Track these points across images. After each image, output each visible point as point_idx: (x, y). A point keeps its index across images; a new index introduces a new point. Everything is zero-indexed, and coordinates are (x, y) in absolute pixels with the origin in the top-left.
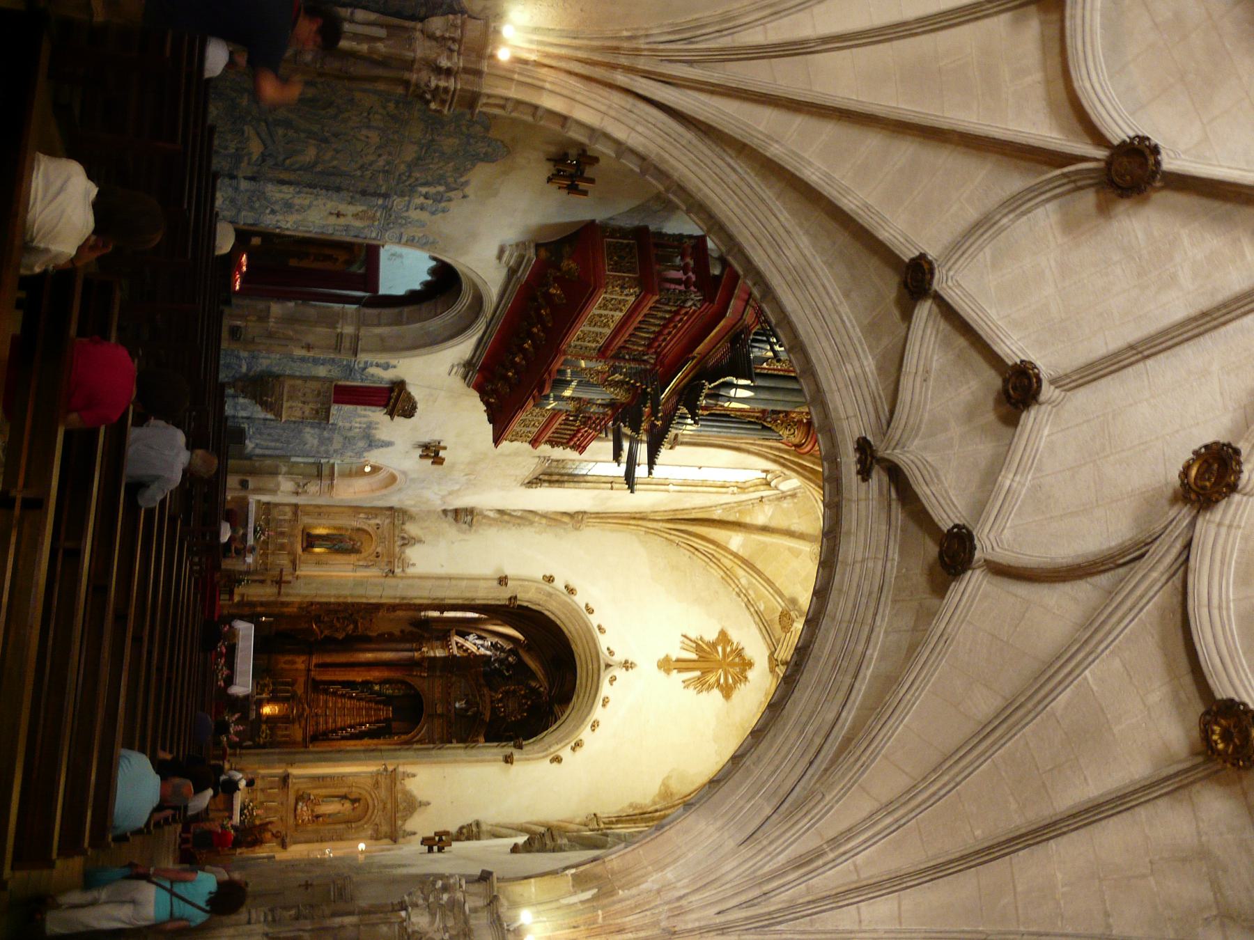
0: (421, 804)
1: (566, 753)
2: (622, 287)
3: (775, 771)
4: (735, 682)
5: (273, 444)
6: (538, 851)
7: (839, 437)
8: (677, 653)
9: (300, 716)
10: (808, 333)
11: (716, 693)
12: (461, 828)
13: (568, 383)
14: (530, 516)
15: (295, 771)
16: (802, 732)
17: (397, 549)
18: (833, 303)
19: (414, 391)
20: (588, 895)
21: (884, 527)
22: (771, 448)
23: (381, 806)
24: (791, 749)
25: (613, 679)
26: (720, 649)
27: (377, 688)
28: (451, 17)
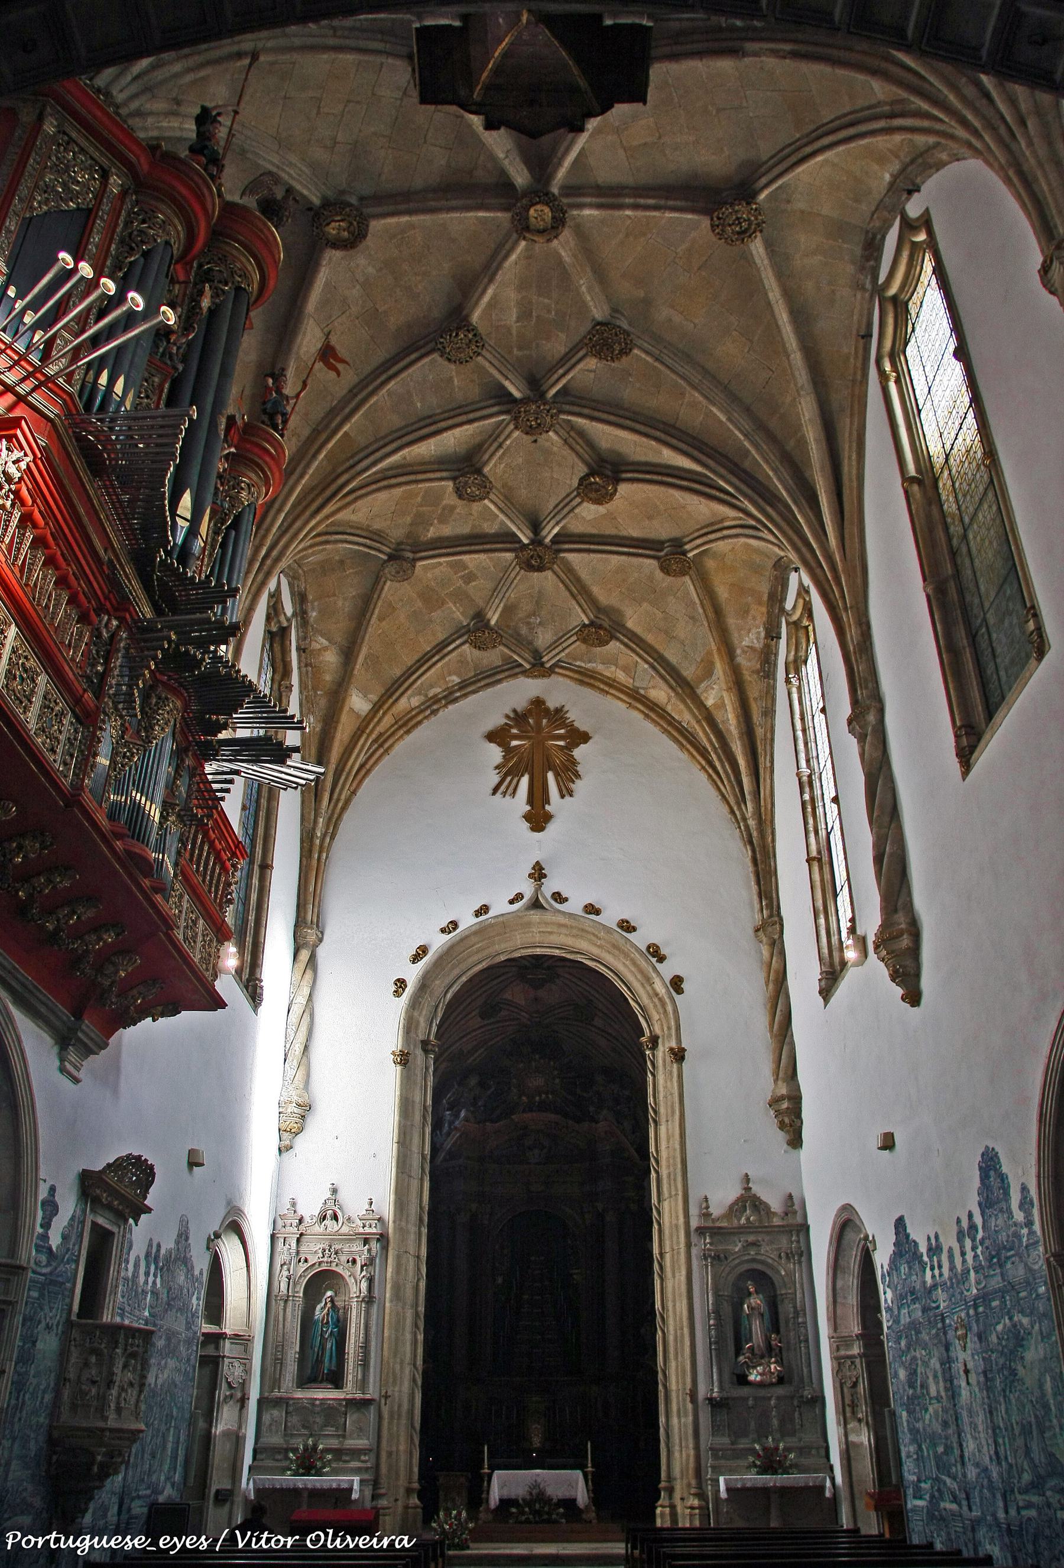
1: (668, 970)
5: (170, 1446)
8: (520, 802)
11: (578, 753)
12: (782, 1126)
13: (137, 807)
17: (345, 1229)
22: (248, 572)
25: (558, 897)
26: (514, 743)
27: (500, 1280)
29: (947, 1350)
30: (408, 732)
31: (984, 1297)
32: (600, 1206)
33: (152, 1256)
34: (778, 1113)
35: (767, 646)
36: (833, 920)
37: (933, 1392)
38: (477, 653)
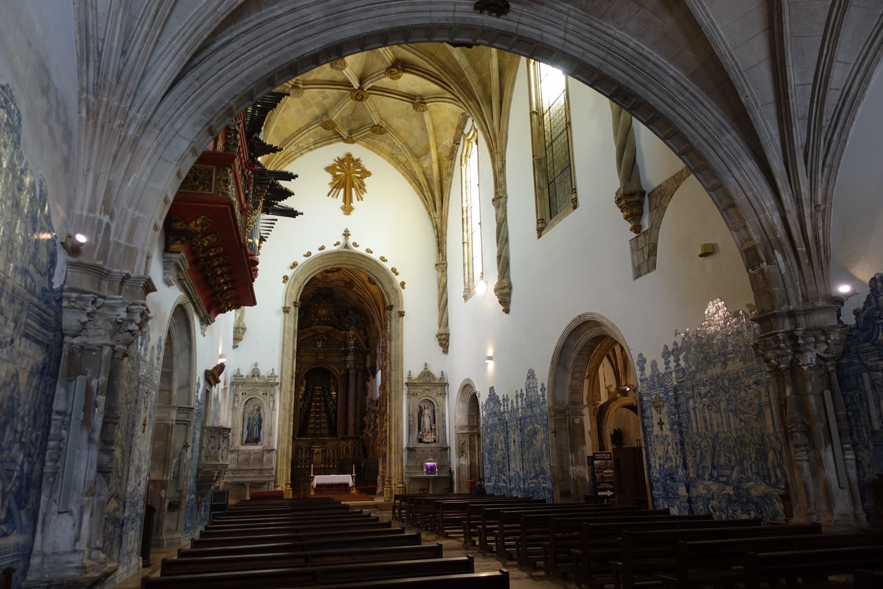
0: (426, 369)
3: (704, 127)
7: (468, 22)
10: (380, 23)
11: (366, 180)
12: (441, 345)
16: (679, 105)
17: (262, 381)
20: (779, 257)
23: (427, 392)
24: (690, 114)
25: (355, 244)
26: (338, 173)
28: (65, 303)
29: (507, 433)
30: (289, 163)
31: (524, 418)
32: (348, 366)
35: (453, 146)
36: (471, 268)
37: (500, 447)
38: (323, 130)
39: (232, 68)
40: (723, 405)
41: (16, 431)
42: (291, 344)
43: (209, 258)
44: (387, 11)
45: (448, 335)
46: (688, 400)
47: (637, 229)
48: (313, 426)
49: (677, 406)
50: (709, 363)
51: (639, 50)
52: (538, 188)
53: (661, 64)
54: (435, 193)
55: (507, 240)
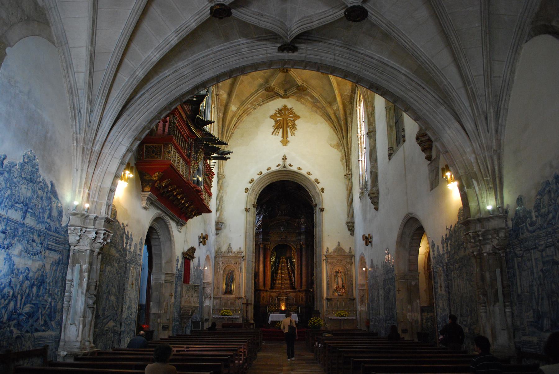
1: (320, 186)
2: (169, 152)
4: (292, 113)
6: (378, 200)
8: (280, 137)
9: (286, 293)
11: (296, 122)
12: (349, 229)
14: (219, 197)
15: (325, 296)
16: (409, 90)
17: (233, 255)
18: (212, 53)
19: (186, 250)
20: (475, 183)
21: (320, 44)
23: (339, 261)
24: (416, 96)
25: (290, 165)
26: (278, 119)
27: (272, 263)
28: (69, 232)
31: (385, 280)
33: (194, 267)
34: (348, 226)
38: (267, 93)
39: (146, 106)
40: (465, 275)
41: (46, 289)
42: (252, 231)
43: (168, 192)
44: (227, 61)
45: (354, 223)
46: (451, 271)
47: (429, 158)
48: (280, 282)
49: (447, 276)
50: (459, 249)
51: (382, 60)
52: (390, 127)
53: (396, 68)
54: (342, 127)
55: (376, 160)
